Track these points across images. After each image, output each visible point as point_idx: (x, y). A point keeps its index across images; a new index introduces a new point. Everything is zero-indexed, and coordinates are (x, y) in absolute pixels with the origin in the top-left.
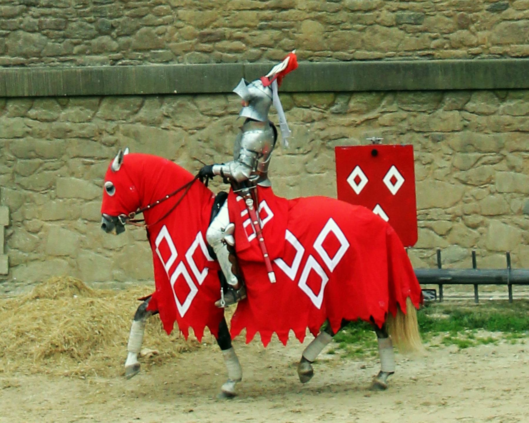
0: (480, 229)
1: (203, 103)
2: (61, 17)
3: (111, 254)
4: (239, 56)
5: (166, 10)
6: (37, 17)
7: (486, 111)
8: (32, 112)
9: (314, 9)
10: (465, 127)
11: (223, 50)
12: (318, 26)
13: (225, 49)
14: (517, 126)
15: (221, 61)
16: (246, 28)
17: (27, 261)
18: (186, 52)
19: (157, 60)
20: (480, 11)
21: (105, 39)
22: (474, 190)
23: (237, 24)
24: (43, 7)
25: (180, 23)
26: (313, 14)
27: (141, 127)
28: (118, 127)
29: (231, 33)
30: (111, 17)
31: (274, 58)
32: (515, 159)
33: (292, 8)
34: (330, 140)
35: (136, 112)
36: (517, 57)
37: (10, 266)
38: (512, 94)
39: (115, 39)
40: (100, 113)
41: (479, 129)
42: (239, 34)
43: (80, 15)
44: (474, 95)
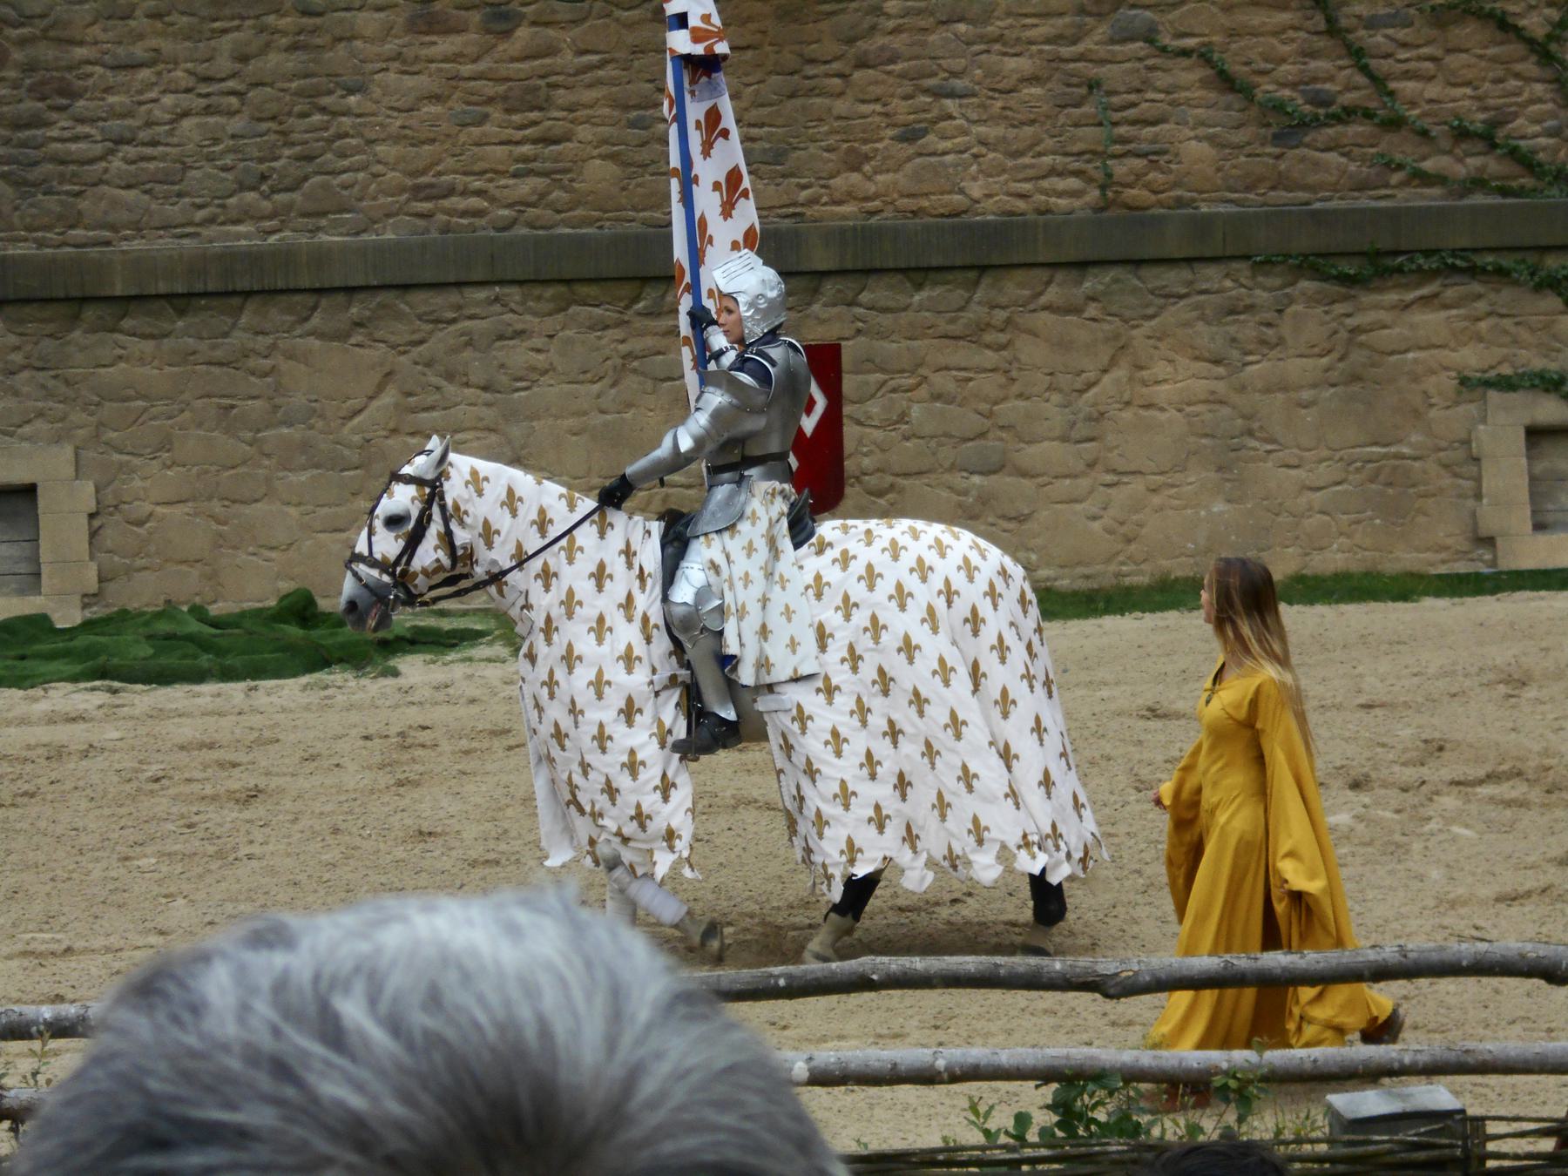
0: (890, 496)
1: (423, 301)
2: (175, 161)
3: (274, 555)
4: (483, 222)
5: (357, 146)
6: (133, 162)
7: (891, 304)
8: (127, 323)
9: (605, 142)
10: (859, 331)
11: (450, 212)
12: (612, 168)
13: (455, 210)
14: (943, 326)
15: (448, 231)
16: (489, 175)
17: (129, 571)
18: (388, 216)
19: (343, 230)
20: (881, 140)
21: (250, 196)
22: (878, 434)
23: (476, 168)
24: (144, 144)
25: (379, 168)
26: (605, 149)
27: (315, 343)
28: (274, 346)
29: (465, 184)
30: (261, 160)
31: (538, 224)
32: (943, 382)
33: (569, 140)
34: (637, 358)
35: (307, 319)
36: (942, 215)
37: (101, 580)
38: (932, 275)
39: (267, 197)
40: (244, 320)
41: (883, 335)
42: (477, 184)
43: (210, 158)
44: (872, 281)
